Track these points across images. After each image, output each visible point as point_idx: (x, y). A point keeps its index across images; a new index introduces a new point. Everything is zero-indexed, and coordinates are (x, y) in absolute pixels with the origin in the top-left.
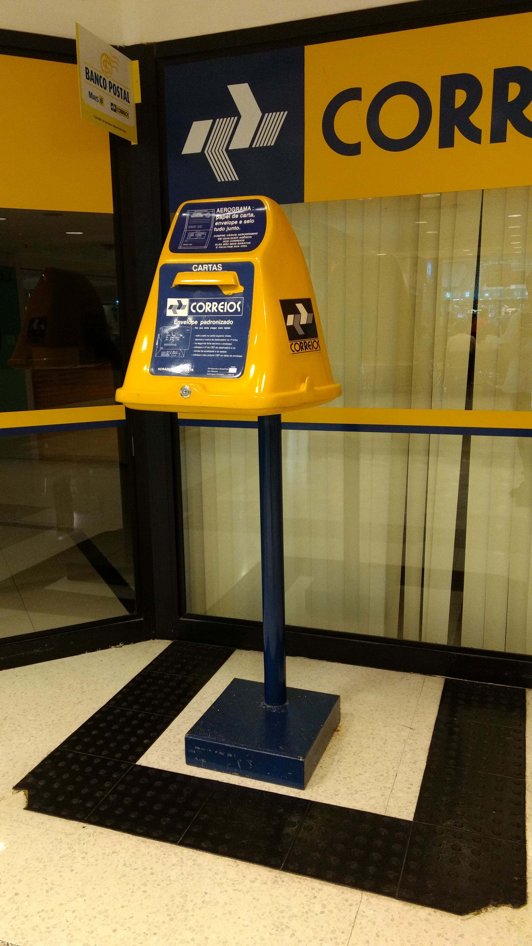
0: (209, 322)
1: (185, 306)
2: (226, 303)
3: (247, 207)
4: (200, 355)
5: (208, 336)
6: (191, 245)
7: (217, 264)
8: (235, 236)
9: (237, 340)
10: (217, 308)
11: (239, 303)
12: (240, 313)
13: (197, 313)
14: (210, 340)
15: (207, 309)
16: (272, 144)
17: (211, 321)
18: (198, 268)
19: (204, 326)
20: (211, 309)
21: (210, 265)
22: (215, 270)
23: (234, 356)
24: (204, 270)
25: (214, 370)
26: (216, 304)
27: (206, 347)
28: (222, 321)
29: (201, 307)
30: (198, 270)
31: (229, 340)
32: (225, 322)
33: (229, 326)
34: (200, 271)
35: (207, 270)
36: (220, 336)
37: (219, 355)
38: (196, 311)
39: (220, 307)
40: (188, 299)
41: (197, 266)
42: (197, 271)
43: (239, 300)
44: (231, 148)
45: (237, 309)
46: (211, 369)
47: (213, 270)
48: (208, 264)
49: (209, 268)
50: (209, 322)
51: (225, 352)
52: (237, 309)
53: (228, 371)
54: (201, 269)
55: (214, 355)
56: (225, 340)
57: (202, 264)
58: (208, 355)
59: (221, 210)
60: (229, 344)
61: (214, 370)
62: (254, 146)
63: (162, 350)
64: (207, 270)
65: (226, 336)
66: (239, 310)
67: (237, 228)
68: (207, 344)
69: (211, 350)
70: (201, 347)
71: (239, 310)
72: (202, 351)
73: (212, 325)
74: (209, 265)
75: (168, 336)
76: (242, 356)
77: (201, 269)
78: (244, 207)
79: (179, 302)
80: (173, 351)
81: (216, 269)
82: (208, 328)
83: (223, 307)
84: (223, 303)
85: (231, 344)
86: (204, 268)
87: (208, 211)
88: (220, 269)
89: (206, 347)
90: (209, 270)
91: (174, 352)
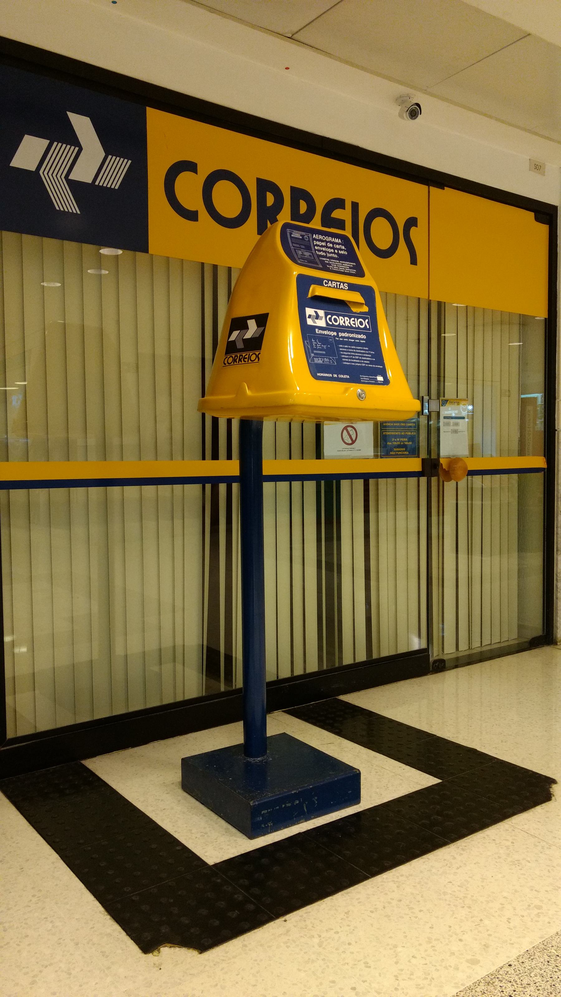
0: (346, 335)
1: (322, 317)
2: (356, 319)
3: (338, 239)
4: (349, 364)
5: (350, 347)
6: (306, 261)
7: (344, 283)
8: (338, 262)
9: (374, 353)
10: (350, 323)
11: (367, 320)
12: (369, 329)
13: (333, 325)
14: (352, 350)
15: (342, 323)
16: (117, 188)
17: (348, 334)
18: (328, 283)
19: (342, 337)
20: (344, 322)
21: (338, 283)
22: (342, 289)
23: (376, 366)
24: (333, 287)
25: (366, 378)
26: (348, 318)
27: (351, 357)
28: (357, 335)
29: (336, 320)
30: (328, 286)
31: (367, 352)
32: (360, 336)
33: (363, 339)
34: (330, 287)
35: (336, 287)
36: (360, 348)
37: (365, 365)
38: (332, 323)
39: (352, 322)
40: (323, 311)
41: (327, 282)
42: (327, 286)
43: (367, 318)
44: (71, 177)
45: (365, 325)
46: (363, 376)
47: (340, 288)
48: (336, 281)
49: (337, 285)
50: (346, 335)
51: (368, 362)
52: (366, 326)
53: (376, 379)
54: (331, 285)
55: (360, 365)
56: (365, 352)
57: (332, 281)
58: (356, 364)
59: (317, 237)
60: (369, 356)
61: (366, 378)
62: (97, 183)
63: (313, 357)
64: (336, 287)
65: (364, 348)
66: (368, 327)
67: (336, 256)
68: (352, 354)
69: (357, 359)
70: (348, 357)
71: (368, 327)
72: (349, 360)
73: (348, 338)
74: (337, 283)
75: (315, 344)
76: (382, 367)
77: (331, 285)
78: (335, 239)
79: (316, 312)
80: (324, 358)
81: (343, 287)
82: (347, 340)
83: (354, 322)
84: (353, 319)
85: (370, 356)
86: (333, 285)
87: (306, 234)
88: (346, 288)
89: (351, 357)
90: (337, 288)
91: (325, 359)
